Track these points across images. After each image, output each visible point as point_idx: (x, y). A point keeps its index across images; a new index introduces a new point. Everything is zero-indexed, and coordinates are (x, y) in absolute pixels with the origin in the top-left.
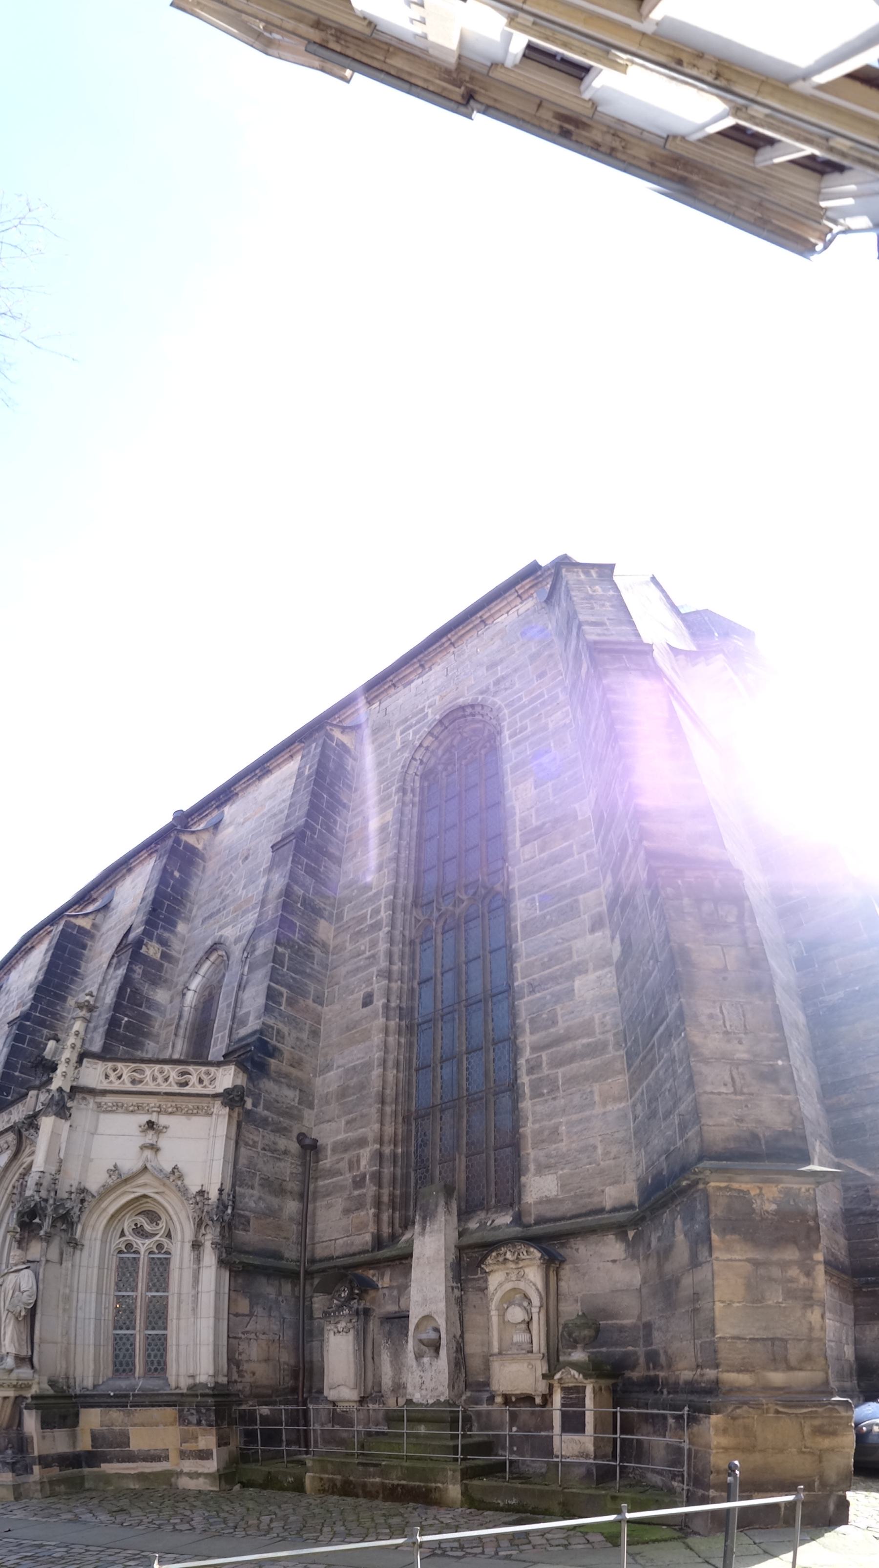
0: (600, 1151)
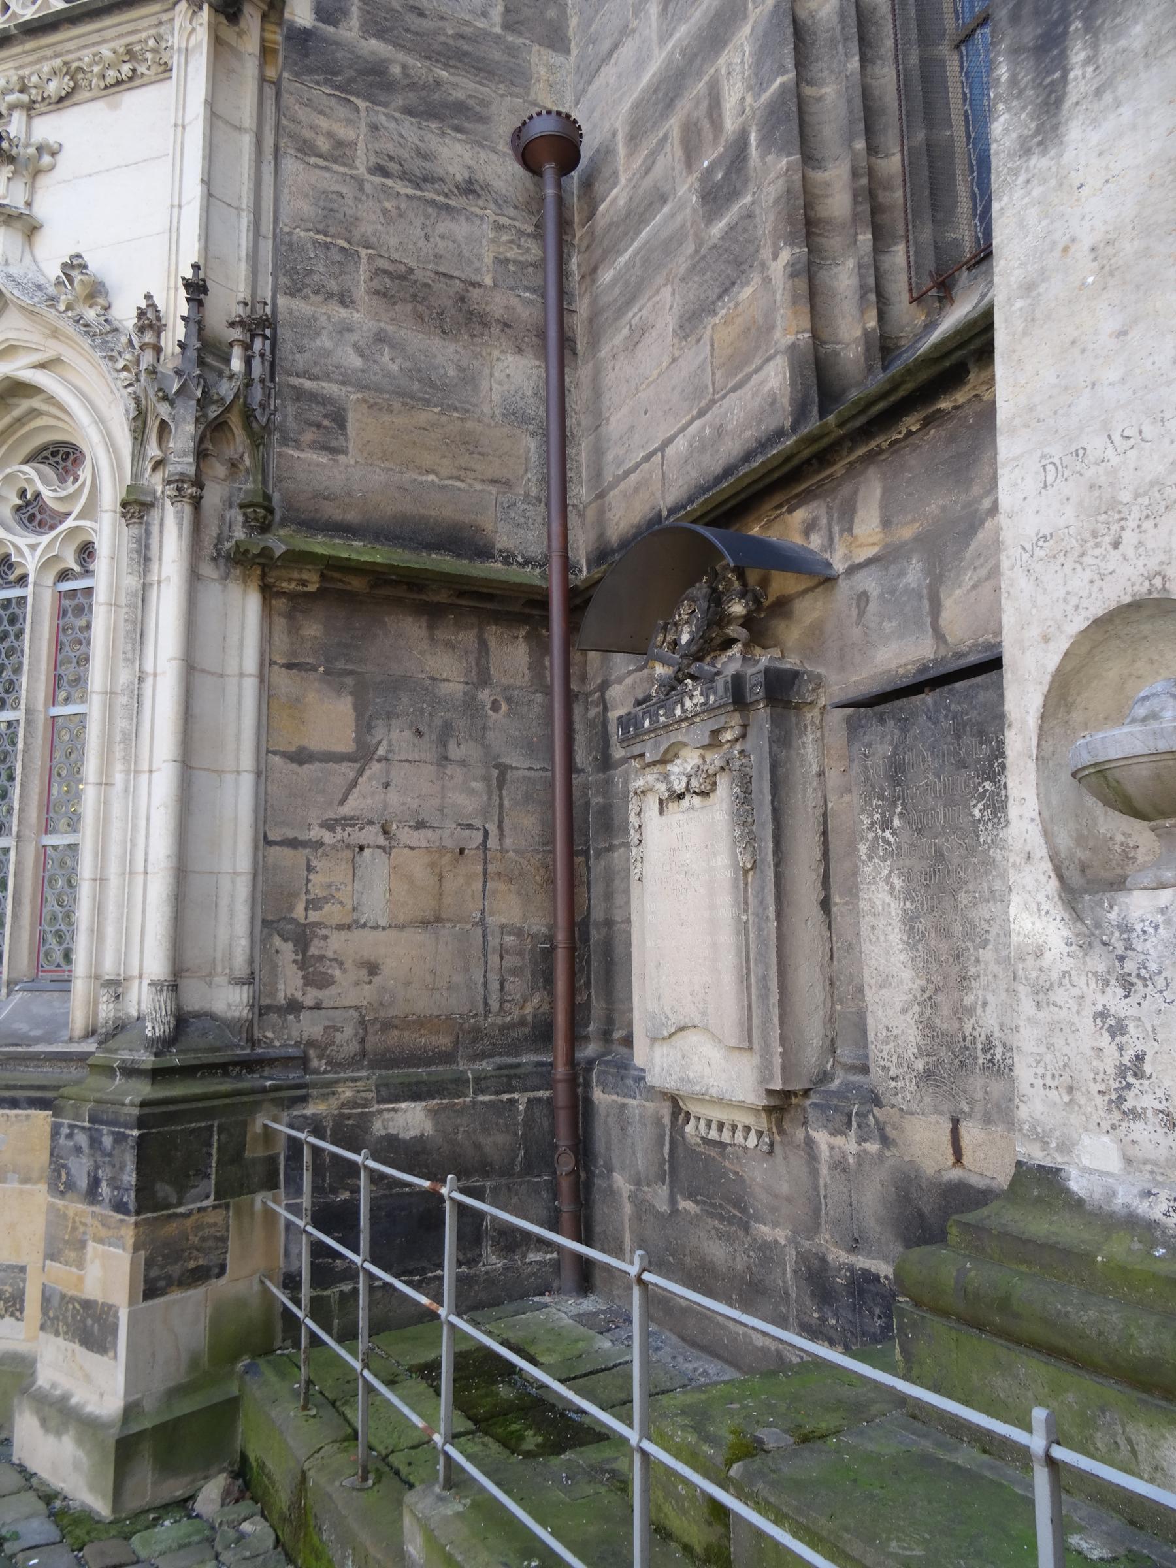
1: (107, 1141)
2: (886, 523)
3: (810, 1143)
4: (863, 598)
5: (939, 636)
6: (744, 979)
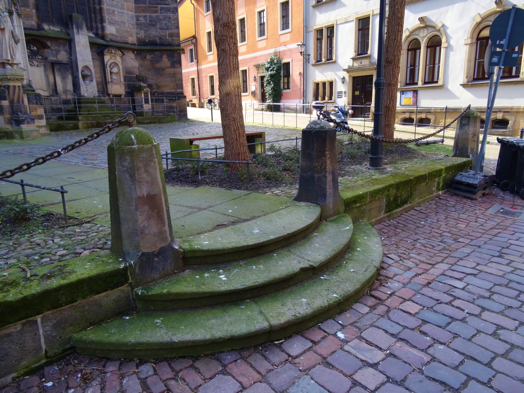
0: (127, 24)
1: (38, 98)
3: (51, 99)
4: (48, 52)
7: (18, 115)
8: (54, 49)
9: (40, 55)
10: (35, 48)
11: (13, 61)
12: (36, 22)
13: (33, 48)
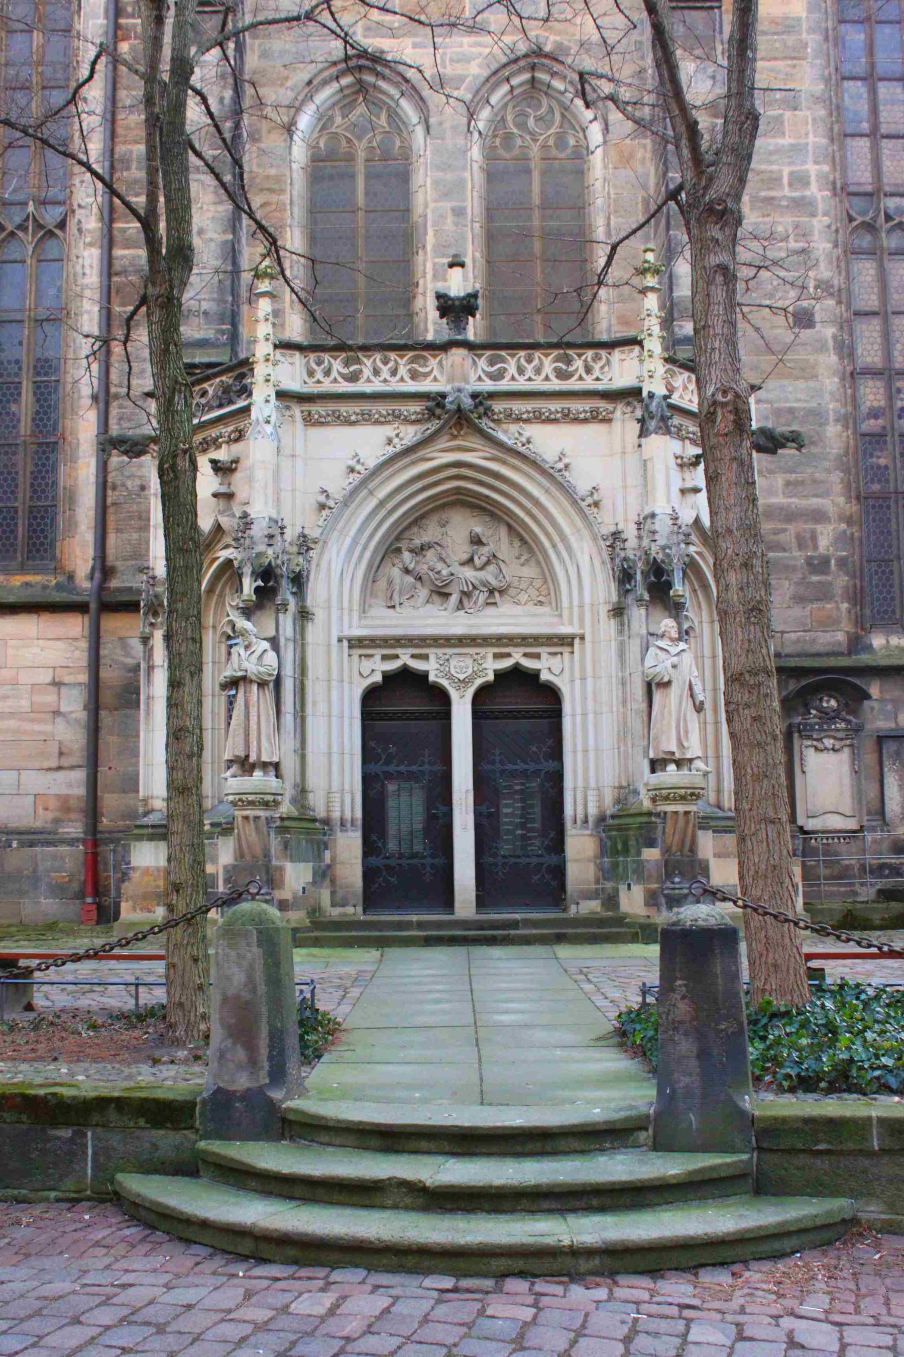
2: (881, 692)
4: (872, 709)
5: (896, 723)
6: (853, 798)
7: (673, 883)
8: (888, 697)
9: (844, 720)
10: (833, 703)
11: (684, 754)
12: (848, 633)
13: (828, 702)
